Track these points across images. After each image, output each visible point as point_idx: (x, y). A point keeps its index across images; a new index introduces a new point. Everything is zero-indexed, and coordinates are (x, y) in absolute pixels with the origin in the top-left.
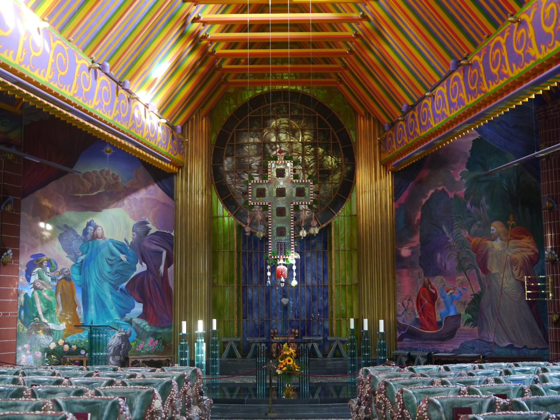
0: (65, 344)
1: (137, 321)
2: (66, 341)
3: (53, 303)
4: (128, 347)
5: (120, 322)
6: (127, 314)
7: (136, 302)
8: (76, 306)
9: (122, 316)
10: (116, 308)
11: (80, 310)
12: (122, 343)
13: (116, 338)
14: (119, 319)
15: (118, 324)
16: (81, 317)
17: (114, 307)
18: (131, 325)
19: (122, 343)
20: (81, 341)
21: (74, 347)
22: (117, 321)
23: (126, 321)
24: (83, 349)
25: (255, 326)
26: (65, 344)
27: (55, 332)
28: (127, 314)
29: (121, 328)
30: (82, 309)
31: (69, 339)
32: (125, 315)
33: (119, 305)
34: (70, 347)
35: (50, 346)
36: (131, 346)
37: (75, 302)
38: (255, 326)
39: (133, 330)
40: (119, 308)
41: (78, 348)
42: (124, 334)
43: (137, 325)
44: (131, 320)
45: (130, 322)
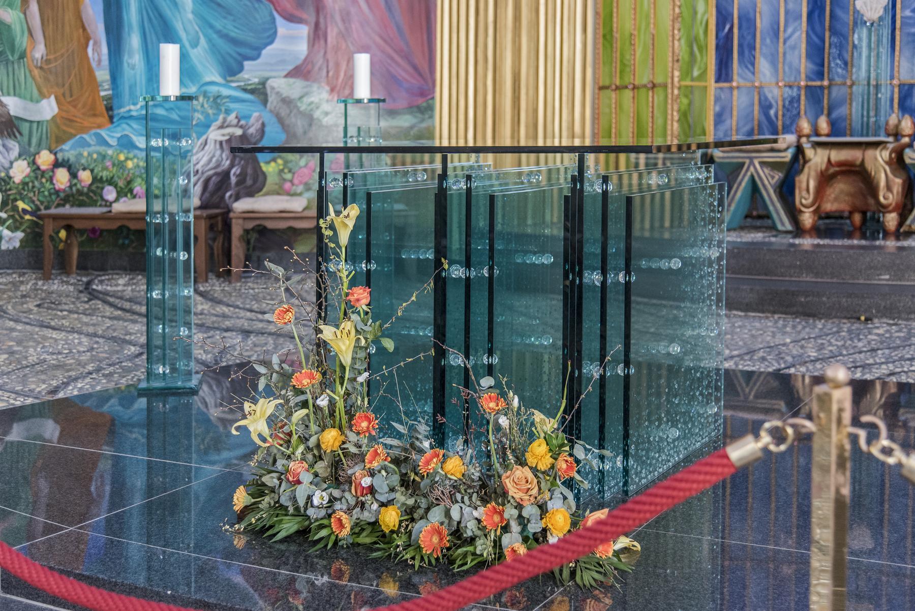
0: (57, 164)
1: (279, 84)
2: (60, 156)
3: (17, 29)
4: (255, 180)
5: (225, 92)
6: (247, 64)
7: (279, 20)
8: (88, 39)
9: (231, 69)
10: (209, 40)
11: (98, 53)
12: (232, 166)
13: (210, 147)
14: (218, 79)
15: (218, 97)
16: (102, 75)
17: (203, 41)
18: (265, 102)
19: (232, 166)
20: (104, 157)
21: (85, 177)
22: (213, 89)
23: (245, 90)
24: (111, 182)
25: (766, 107)
26: (57, 164)
27: (25, 128)
28: (247, 64)
29: (228, 112)
30: (105, 50)
31: (68, 151)
32: (241, 69)
33: (218, 32)
34: (74, 175)
35: (12, 173)
36: (264, 175)
37: (84, 29)
38: (766, 107)
39: (267, 117)
40: (220, 42)
41: (95, 179)
42: (239, 132)
43: (287, 101)
44: (263, 83)
45: (260, 92)
